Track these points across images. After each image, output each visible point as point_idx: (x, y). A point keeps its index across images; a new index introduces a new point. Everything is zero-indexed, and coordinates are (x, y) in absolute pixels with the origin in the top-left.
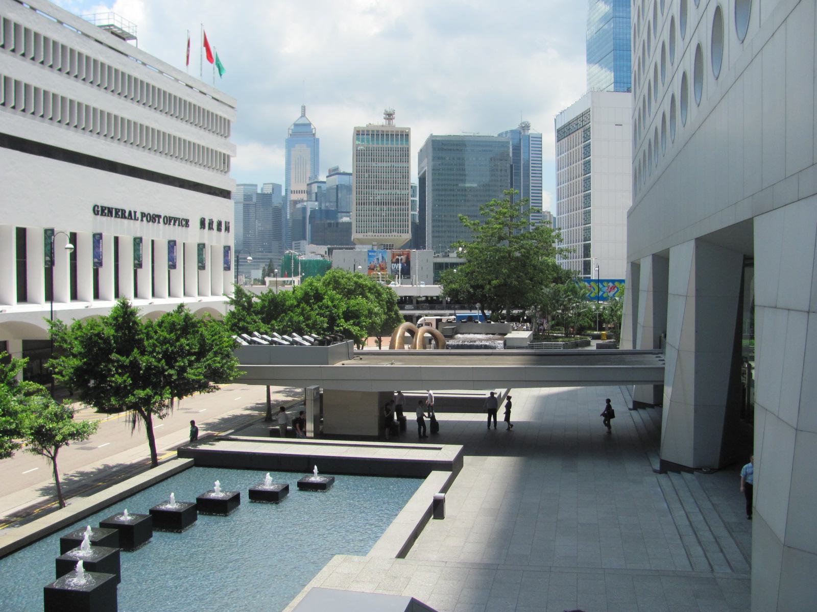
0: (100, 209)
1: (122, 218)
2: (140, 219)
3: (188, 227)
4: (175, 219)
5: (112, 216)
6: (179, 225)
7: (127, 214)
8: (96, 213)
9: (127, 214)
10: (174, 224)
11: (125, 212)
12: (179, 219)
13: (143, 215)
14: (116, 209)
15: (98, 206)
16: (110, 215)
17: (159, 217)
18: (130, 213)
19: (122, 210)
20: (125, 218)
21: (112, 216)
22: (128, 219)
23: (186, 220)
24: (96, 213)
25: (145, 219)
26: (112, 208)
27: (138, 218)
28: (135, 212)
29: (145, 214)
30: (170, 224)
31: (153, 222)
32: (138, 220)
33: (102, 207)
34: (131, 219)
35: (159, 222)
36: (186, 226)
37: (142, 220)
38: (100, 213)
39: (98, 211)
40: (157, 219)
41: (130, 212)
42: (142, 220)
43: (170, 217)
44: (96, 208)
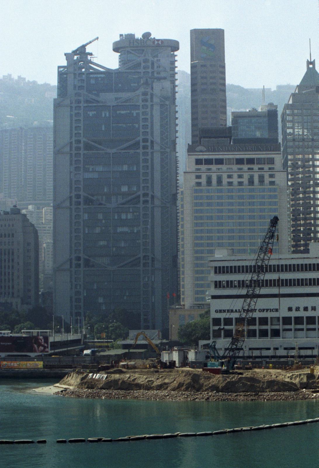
0: (219, 311)
4: (267, 310)
6: (270, 311)
7: (234, 311)
9: (234, 311)
10: (267, 311)
11: (233, 310)
12: (270, 309)
20: (233, 312)
22: (235, 312)
26: (225, 310)
30: (263, 312)
33: (220, 310)
34: (237, 312)
35: (255, 312)
36: (276, 311)
44: (217, 311)
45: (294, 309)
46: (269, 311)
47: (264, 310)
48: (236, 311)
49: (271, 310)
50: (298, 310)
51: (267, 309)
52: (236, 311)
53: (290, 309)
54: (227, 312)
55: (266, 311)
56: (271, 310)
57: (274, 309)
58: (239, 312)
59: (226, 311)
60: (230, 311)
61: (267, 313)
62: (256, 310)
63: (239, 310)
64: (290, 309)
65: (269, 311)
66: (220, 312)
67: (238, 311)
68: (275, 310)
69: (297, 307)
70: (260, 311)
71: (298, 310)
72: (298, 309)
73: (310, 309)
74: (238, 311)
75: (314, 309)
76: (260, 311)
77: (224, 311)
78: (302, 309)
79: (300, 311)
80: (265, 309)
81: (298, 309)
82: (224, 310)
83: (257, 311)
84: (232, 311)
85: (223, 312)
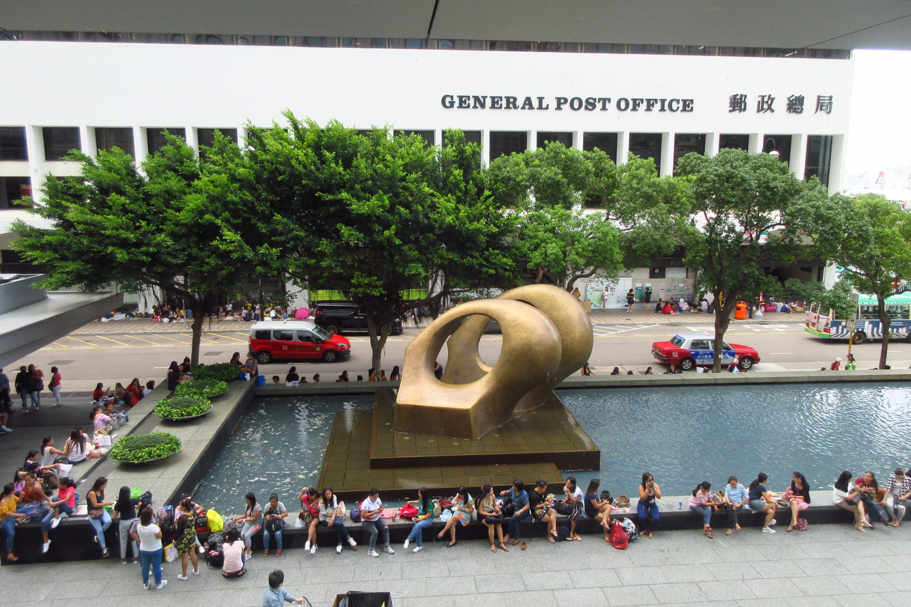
0: (456, 100)
1: (508, 107)
2: (553, 104)
3: (692, 110)
4: (650, 104)
5: (483, 106)
6: (662, 109)
7: (520, 103)
8: (448, 105)
9: (520, 103)
11: (515, 99)
12: (663, 101)
13: (560, 102)
14: (493, 98)
15: (452, 97)
16: (478, 105)
17: (605, 101)
18: (528, 101)
19: (508, 98)
20: (515, 107)
21: (483, 106)
22: (523, 108)
23: (685, 101)
24: (448, 105)
25: (566, 107)
26: (484, 98)
27: (548, 105)
28: (541, 100)
29: (566, 100)
30: (634, 109)
31: (586, 108)
32: (547, 108)
33: (460, 98)
34: (531, 107)
35: (604, 108)
36: (684, 110)
37: (559, 108)
38: (457, 104)
39: (452, 104)
40: (599, 106)
41: (528, 101)
42: (559, 108)
43: (634, 100)
44: (448, 100)
45: (752, 103)
46: (658, 106)
47: (636, 103)
48: (528, 102)
49: (667, 106)
50: (766, 106)
51: (648, 101)
52: (528, 102)
53: (738, 103)
54: (493, 107)
55: (644, 106)
56: (667, 106)
57: (678, 101)
58: (540, 107)
59: (488, 103)
60: (504, 103)
61: (648, 113)
62: (609, 100)
63: (541, 100)
64: (738, 103)
65: (658, 106)
66: (460, 106)
67: (535, 104)
68: (681, 105)
69: (763, 97)
70: (623, 105)
71: (766, 106)
72: (766, 104)
73: (810, 104)
74: (535, 104)
75: (823, 105)
76: (623, 105)
77: (480, 102)
78: (780, 105)
79: (773, 111)
80: (642, 100)
81: (766, 104)
82: (476, 99)
83: (611, 106)
84: (511, 103)
85: (475, 107)
